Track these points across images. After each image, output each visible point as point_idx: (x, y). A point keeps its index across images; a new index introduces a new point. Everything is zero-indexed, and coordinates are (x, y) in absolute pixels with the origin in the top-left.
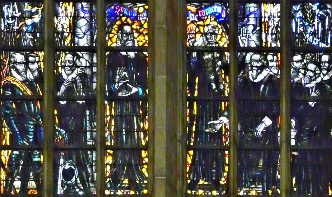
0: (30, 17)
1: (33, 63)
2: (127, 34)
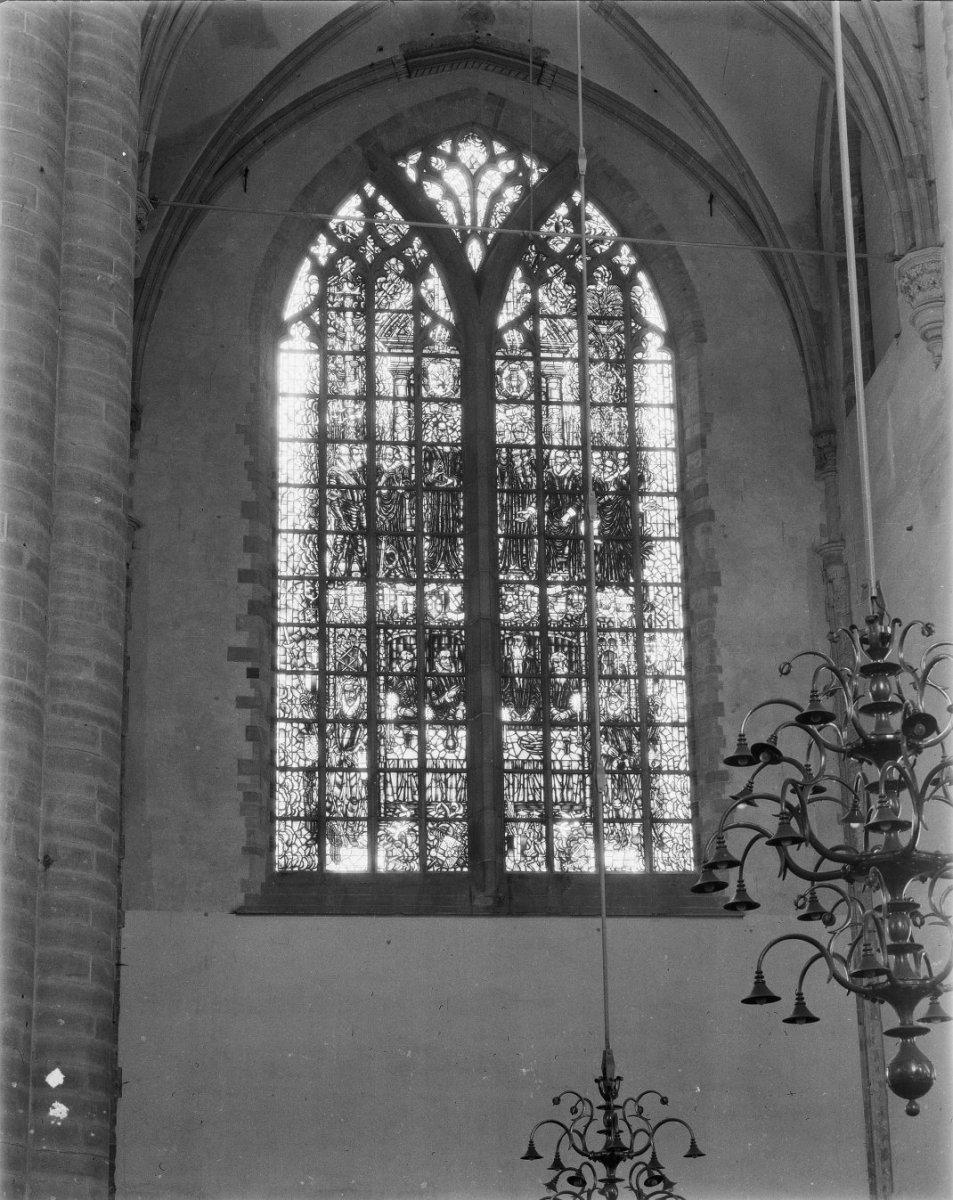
1: (357, 454)
2: (442, 431)
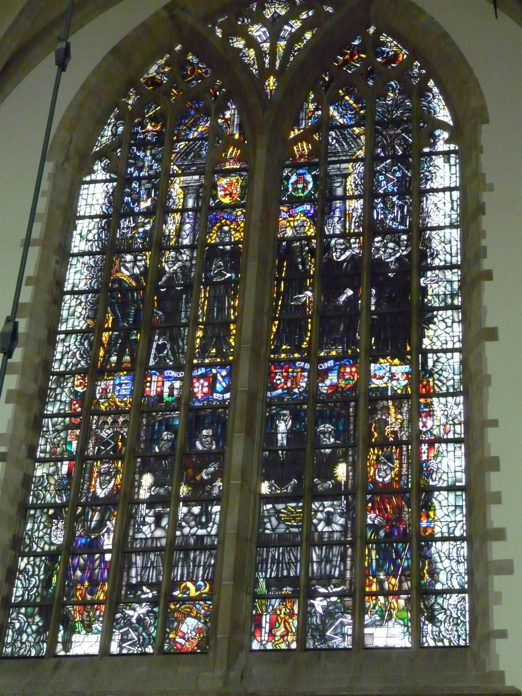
0: (143, 226)
1: (140, 261)
2: (226, 232)
